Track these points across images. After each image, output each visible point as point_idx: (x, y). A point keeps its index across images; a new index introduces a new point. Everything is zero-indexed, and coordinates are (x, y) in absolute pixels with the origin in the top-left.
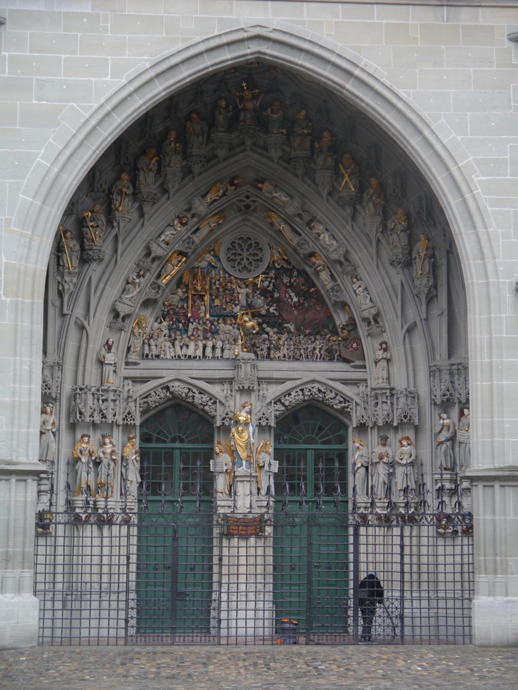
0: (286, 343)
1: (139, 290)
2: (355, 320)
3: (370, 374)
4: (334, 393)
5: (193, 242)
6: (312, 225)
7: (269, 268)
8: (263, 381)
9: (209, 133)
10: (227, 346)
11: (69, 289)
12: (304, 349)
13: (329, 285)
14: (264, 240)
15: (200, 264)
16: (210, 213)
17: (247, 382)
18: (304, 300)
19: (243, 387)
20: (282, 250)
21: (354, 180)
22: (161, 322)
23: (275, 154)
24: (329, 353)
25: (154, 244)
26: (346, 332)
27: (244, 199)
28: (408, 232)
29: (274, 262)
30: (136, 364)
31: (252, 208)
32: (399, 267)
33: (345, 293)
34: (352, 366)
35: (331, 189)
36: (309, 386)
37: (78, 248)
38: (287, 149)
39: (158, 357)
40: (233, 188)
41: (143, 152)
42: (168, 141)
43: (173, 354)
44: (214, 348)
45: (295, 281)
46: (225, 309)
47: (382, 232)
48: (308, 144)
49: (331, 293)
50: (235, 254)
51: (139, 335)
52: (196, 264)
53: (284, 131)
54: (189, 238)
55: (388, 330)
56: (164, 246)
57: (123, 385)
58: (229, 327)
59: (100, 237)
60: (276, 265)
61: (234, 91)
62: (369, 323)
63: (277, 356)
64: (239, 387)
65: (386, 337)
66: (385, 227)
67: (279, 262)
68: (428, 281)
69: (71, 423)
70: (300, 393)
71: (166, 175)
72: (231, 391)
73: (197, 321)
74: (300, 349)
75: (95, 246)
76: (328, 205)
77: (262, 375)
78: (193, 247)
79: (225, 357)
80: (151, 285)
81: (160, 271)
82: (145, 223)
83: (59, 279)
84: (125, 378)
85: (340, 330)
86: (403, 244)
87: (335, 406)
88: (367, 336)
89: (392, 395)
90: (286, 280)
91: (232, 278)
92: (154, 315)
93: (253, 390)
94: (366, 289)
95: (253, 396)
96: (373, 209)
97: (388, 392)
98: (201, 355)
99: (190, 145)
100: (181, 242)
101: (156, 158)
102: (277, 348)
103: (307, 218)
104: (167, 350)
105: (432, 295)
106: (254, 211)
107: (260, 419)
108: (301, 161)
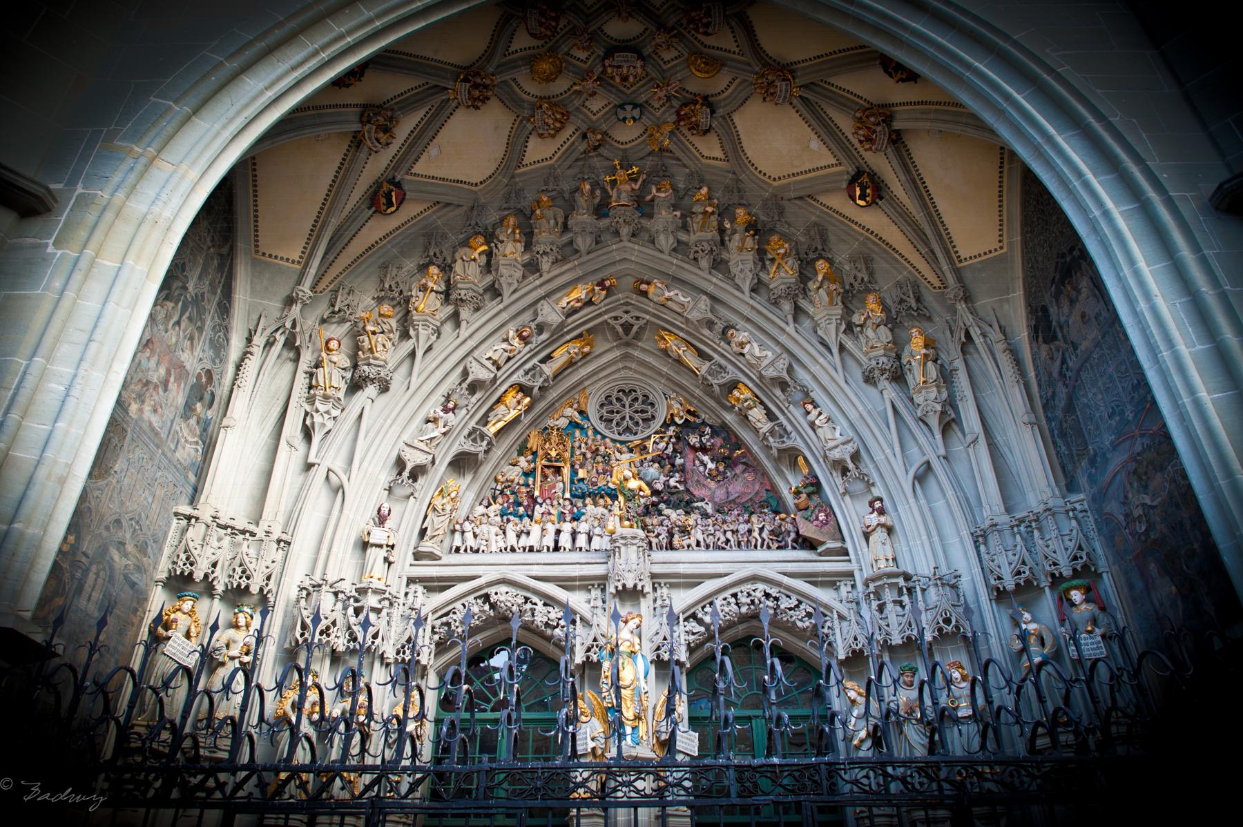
0: (699, 521)
1: (444, 430)
2: (817, 478)
3: (858, 561)
4: (794, 597)
5: (542, 373)
6: (730, 332)
7: (666, 425)
8: (662, 581)
10: (598, 531)
11: (323, 425)
12: (733, 532)
13: (765, 427)
14: (657, 391)
15: (557, 423)
17: (632, 575)
18: (725, 468)
19: (624, 586)
20: (685, 399)
21: (790, 262)
22: (490, 505)
23: (666, 242)
24: (778, 536)
25: (474, 363)
26: (804, 496)
28: (890, 326)
29: (672, 415)
30: (432, 557)
31: (635, 329)
32: (882, 378)
33: (794, 434)
34: (820, 555)
35: (756, 281)
36: (748, 587)
37: (347, 363)
38: (683, 237)
39: (477, 551)
40: (604, 292)
41: (465, 243)
43: (502, 545)
44: (574, 535)
45: (708, 440)
46: (594, 484)
47: (845, 332)
48: (715, 224)
49: (771, 439)
50: (612, 412)
51: (443, 510)
52: (551, 423)
53: (678, 213)
54: (534, 367)
55: (878, 483)
56: (493, 368)
57: (406, 594)
58: (600, 510)
59: (384, 346)
60: (677, 419)
62: (845, 471)
63: (685, 543)
64: (617, 587)
65: (876, 492)
66: (850, 329)
67: (682, 414)
68: (939, 392)
69: (286, 649)
70: (733, 600)
71: (497, 270)
72: (604, 602)
73: (548, 501)
74: (725, 532)
75: (376, 359)
76: (752, 302)
77: (657, 569)
78: (542, 379)
79: (593, 546)
80: (469, 435)
81: (486, 415)
82: (461, 333)
83: (308, 408)
84: (411, 581)
85: (790, 500)
86: (885, 341)
87: (799, 624)
88: (844, 494)
89: (910, 591)
90: (694, 440)
91: (607, 440)
92: (476, 487)
93: (642, 594)
94: (829, 419)
95: (645, 605)
96: (826, 299)
97: (901, 581)
98: (552, 545)
100: (521, 372)
101: (484, 248)
102: (685, 531)
103: (719, 326)
104: (493, 538)
105: (948, 419)
106: (637, 337)
107: (658, 648)
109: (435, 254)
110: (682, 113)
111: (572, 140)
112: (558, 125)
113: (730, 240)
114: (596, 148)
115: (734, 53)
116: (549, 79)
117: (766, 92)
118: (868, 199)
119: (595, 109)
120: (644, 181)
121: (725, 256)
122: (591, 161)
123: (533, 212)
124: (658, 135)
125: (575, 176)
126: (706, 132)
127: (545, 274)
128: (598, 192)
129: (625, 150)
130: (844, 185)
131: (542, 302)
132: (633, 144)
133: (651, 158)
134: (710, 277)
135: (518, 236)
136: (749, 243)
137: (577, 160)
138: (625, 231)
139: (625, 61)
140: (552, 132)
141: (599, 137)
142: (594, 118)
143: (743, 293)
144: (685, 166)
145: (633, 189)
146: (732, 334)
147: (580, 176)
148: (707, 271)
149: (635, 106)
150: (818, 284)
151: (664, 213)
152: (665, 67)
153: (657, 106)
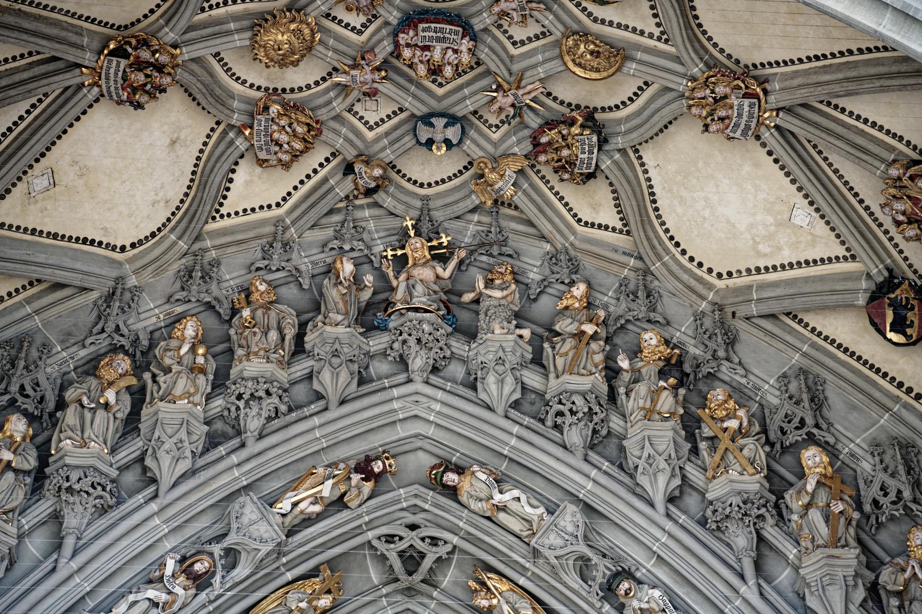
6: (625, 585)
9: (300, 338)
16: (290, 566)
27: (403, 532)
31: (427, 563)
35: (677, 482)
38: (533, 379)
40: (368, 487)
42: (174, 343)
48: (599, 358)
53: (526, 333)
61: (381, 248)
76: (669, 525)
82: (63, 561)
99: (240, 352)
103: (602, 570)
108: (579, 401)
109: (22, 388)
110: (544, 140)
111: (322, 173)
112: (298, 146)
113: (627, 394)
114: (369, 192)
115: (651, 36)
116: (285, 61)
117: (711, 114)
118: (909, 331)
119: (372, 118)
120: (461, 262)
121: (616, 423)
122: (359, 214)
123: (235, 312)
124: (493, 176)
125: (325, 245)
126: (590, 176)
127: (250, 442)
128: (369, 279)
129: (426, 199)
130: (862, 300)
131: (241, 499)
132: (442, 187)
133: (476, 217)
134: (586, 468)
135: (200, 360)
136: (666, 402)
137: (331, 212)
138: (418, 361)
139: (439, 40)
140: (286, 157)
141: (378, 172)
142: (370, 135)
143: (652, 505)
144: (543, 237)
145: (438, 277)
146: (627, 594)
147: (335, 244)
148: (580, 453)
149: (452, 120)
150: (806, 499)
151: (498, 331)
152: (514, 51)
153: (493, 120)
